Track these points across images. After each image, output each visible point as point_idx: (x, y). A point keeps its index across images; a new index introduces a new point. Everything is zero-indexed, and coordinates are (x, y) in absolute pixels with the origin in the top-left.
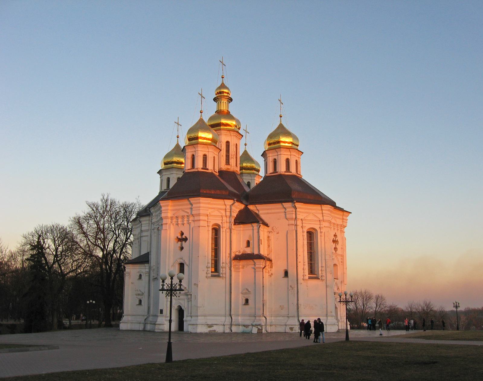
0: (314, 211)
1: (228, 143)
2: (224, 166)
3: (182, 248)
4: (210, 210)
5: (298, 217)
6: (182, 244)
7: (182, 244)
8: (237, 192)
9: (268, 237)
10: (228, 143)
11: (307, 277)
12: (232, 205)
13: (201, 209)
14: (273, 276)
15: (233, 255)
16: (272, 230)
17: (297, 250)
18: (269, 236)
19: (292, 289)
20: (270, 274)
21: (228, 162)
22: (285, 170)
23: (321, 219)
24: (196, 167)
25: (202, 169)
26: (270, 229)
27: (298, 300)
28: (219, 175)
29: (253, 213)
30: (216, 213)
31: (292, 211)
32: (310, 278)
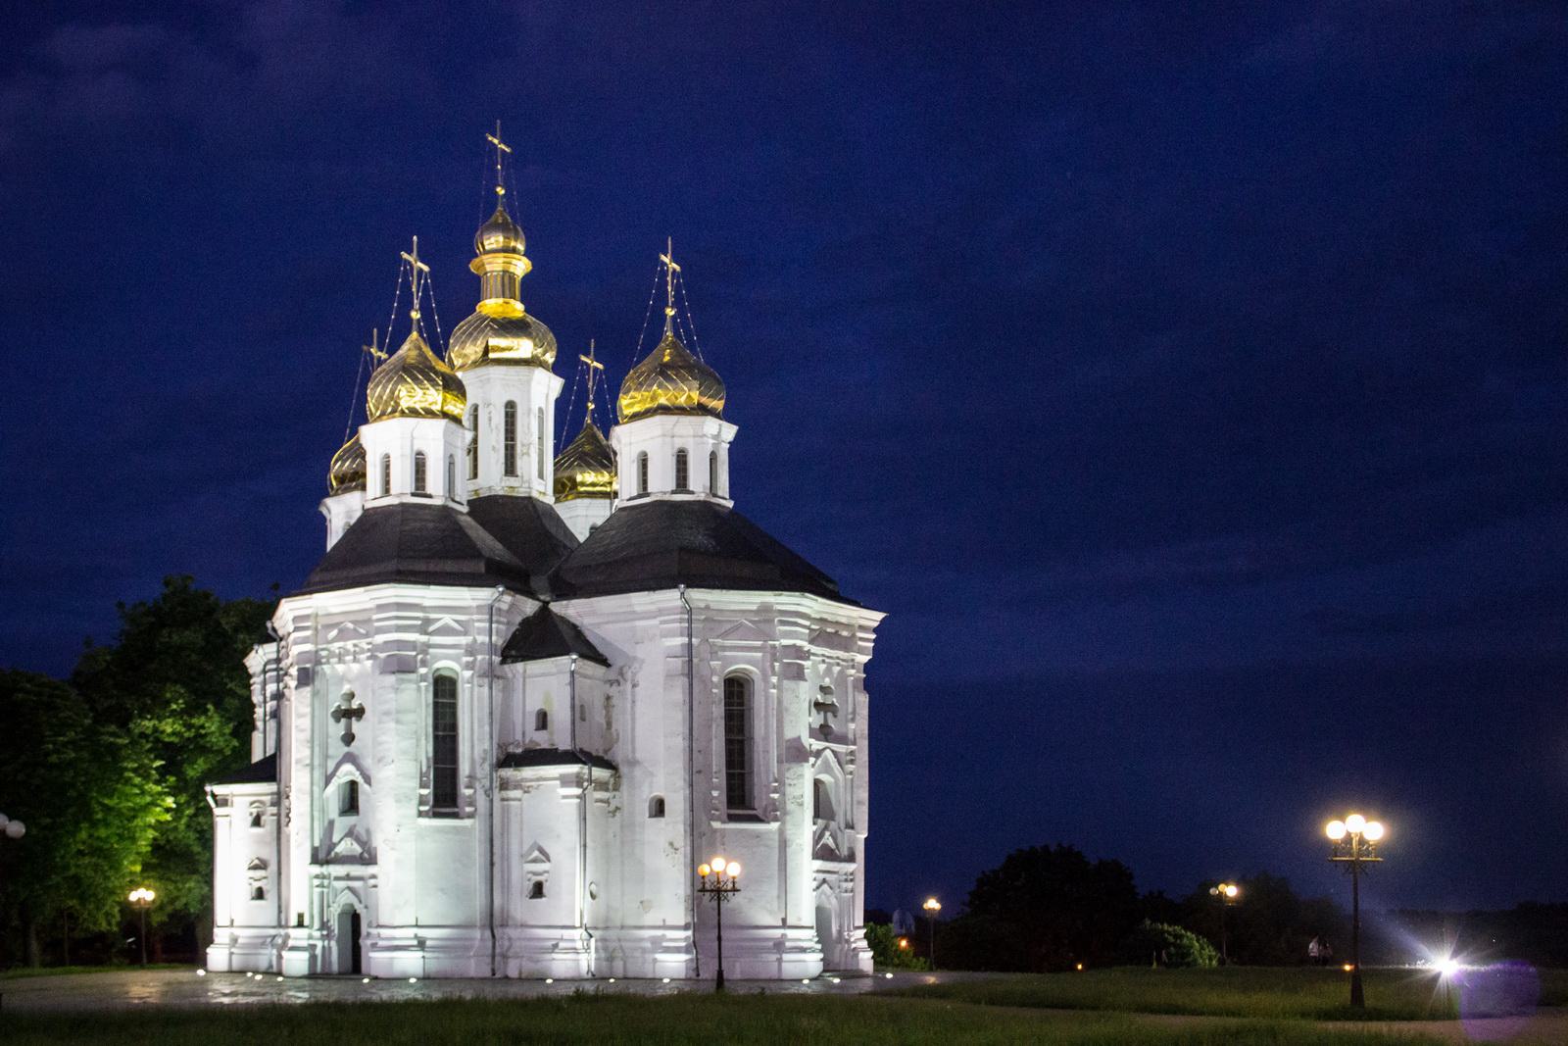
2: (498, 481)
3: (349, 738)
6: (349, 727)
7: (349, 727)
9: (608, 698)
16: (620, 678)
18: (611, 694)
19: (673, 851)
20: (612, 807)
21: (510, 469)
22: (672, 486)
24: (394, 488)
26: (612, 674)
28: (469, 514)
29: (563, 628)
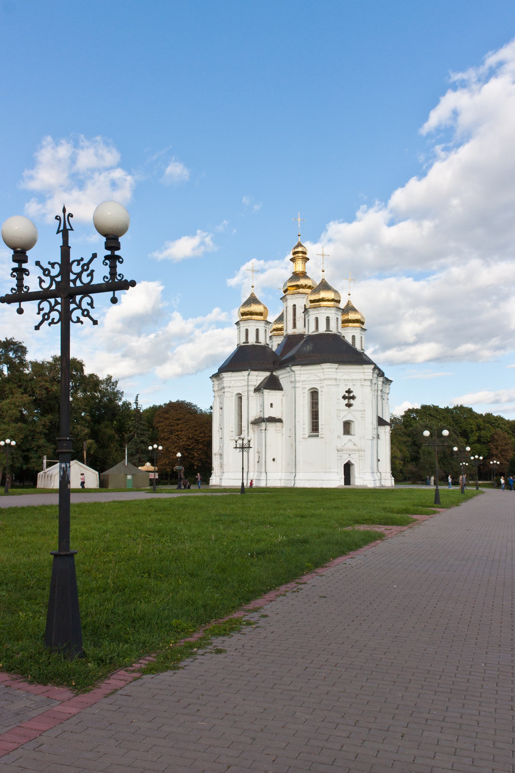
0: (315, 371)
1: (294, 306)
4: (233, 382)
5: (297, 379)
8: (283, 358)
10: (294, 306)
11: (307, 436)
12: (248, 375)
13: (224, 382)
14: (284, 435)
15: (252, 419)
17: (295, 410)
21: (295, 326)
23: (323, 378)
25: (244, 343)
27: (295, 457)
30: (238, 384)
31: (292, 375)
32: (310, 436)
